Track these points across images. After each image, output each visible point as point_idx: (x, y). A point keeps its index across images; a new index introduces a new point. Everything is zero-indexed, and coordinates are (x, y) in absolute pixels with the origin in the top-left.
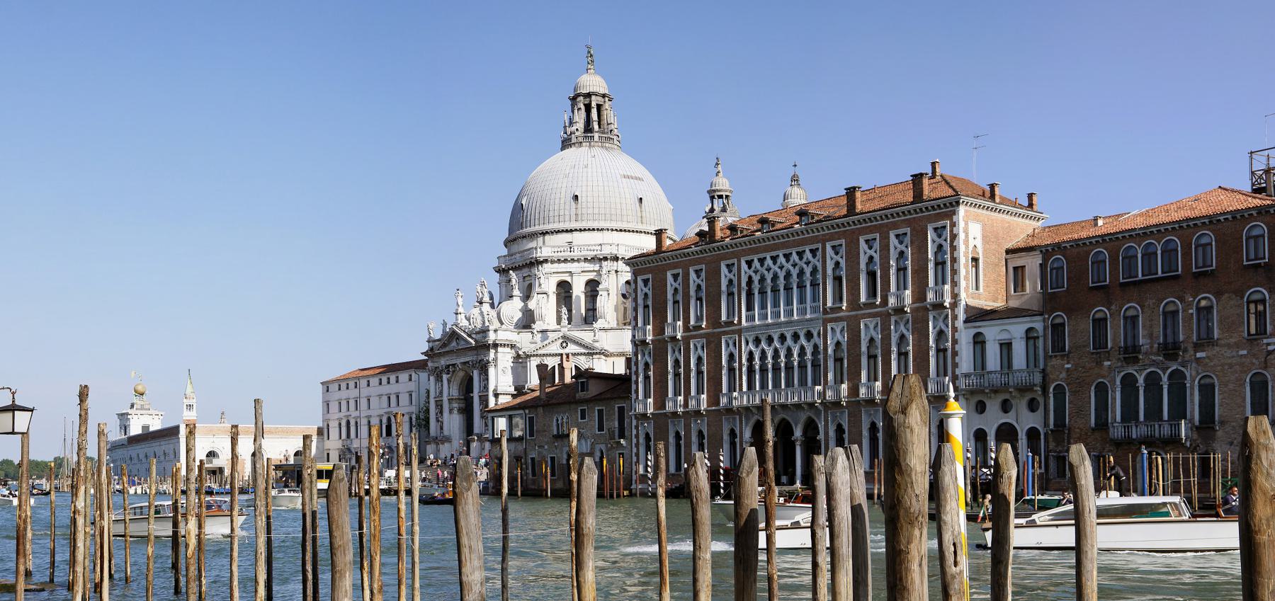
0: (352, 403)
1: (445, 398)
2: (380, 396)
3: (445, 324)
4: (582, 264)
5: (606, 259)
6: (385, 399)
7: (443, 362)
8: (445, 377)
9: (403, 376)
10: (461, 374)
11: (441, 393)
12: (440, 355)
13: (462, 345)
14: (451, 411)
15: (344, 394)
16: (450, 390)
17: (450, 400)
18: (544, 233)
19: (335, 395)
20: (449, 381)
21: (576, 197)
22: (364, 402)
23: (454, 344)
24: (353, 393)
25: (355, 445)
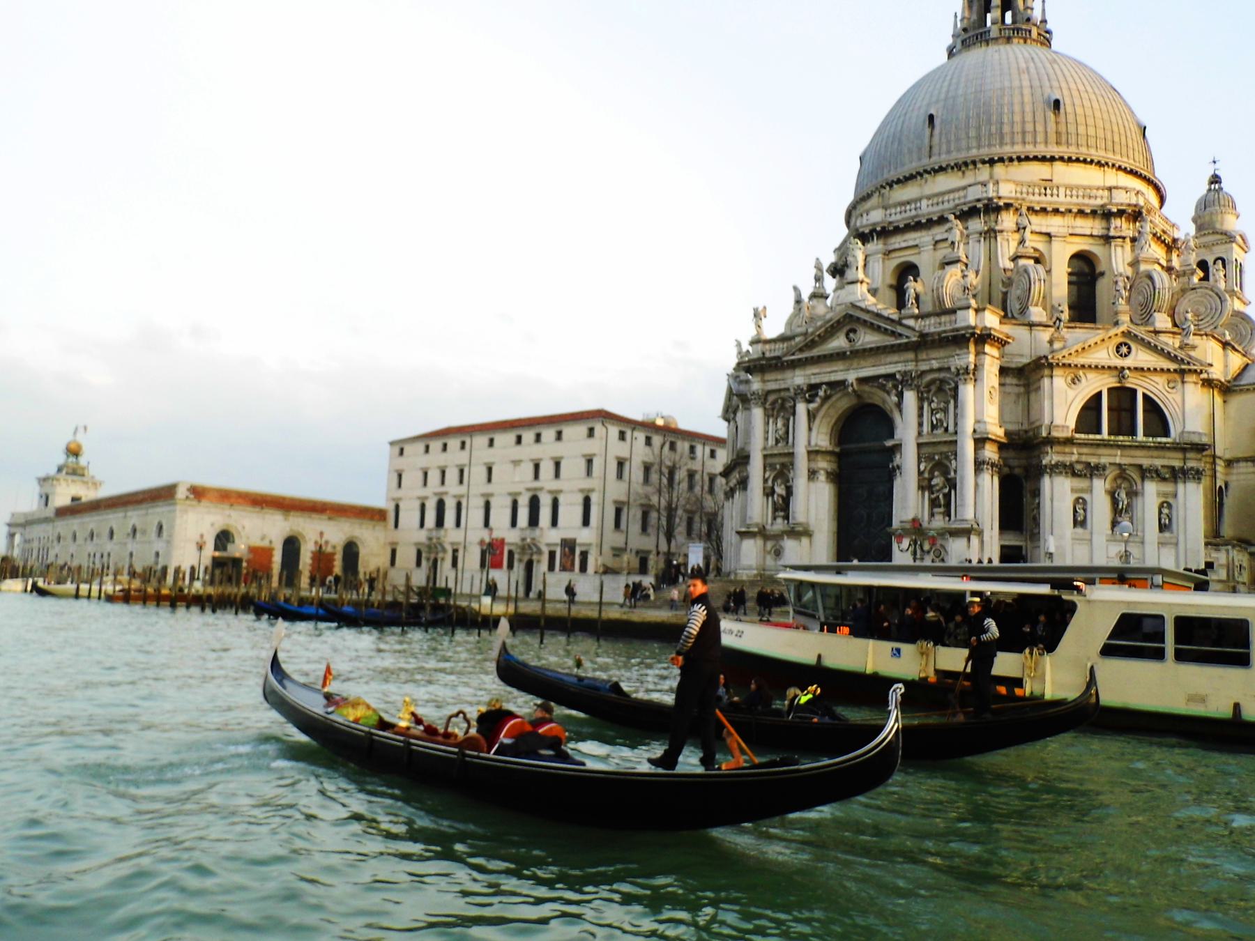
0: (452, 475)
2: (516, 463)
4: (1069, 220)
5: (1121, 213)
7: (799, 378)
8: (801, 408)
9: (574, 432)
10: (843, 404)
12: (794, 365)
13: (867, 339)
14: (812, 474)
15: (436, 458)
16: (811, 434)
17: (813, 454)
18: (992, 162)
20: (811, 416)
21: (1057, 104)
22: (478, 473)
23: (839, 342)
24: (455, 456)
25: (450, 535)
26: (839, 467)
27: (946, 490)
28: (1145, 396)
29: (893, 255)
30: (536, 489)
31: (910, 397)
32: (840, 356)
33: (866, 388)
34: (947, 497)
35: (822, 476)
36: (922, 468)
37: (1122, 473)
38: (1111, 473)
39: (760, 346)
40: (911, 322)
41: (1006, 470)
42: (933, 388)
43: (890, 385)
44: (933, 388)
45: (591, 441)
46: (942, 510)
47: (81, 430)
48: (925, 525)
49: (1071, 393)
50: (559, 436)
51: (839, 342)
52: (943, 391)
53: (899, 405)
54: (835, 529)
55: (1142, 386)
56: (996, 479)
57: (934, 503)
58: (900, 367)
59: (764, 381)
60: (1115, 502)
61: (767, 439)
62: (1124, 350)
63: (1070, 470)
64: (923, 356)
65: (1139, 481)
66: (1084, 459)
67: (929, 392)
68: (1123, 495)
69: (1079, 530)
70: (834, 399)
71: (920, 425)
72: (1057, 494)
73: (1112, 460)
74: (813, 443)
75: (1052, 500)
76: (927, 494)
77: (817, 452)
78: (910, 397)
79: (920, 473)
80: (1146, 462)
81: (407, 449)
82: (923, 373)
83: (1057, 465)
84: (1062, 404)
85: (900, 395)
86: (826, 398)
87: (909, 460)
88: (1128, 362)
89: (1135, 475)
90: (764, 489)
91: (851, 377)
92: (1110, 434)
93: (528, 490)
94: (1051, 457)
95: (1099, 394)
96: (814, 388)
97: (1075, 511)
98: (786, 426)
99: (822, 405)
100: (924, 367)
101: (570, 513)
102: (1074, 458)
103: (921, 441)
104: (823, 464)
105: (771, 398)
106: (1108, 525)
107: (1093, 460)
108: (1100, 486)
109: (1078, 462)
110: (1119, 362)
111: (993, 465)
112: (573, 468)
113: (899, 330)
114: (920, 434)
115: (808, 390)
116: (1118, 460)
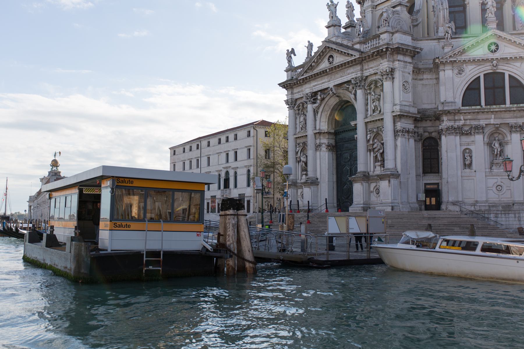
1: (310, 132)
3: (310, 46)
6: (224, 156)
7: (308, 89)
8: (310, 107)
10: (333, 101)
11: (304, 127)
13: (338, 59)
14: (318, 147)
15: (188, 155)
17: (318, 134)
19: (181, 156)
20: (315, 112)
22: (204, 161)
23: (324, 65)
26: (336, 141)
27: (381, 151)
28: (510, 76)
29: (378, 8)
30: (227, 168)
31: (360, 93)
32: (324, 73)
33: (341, 91)
34: (382, 154)
35: (324, 148)
36: (368, 138)
37: (497, 129)
38: (488, 131)
39: (290, 72)
40: (357, 46)
41: (426, 135)
42: (373, 86)
43: (351, 87)
44: (373, 86)
45: (249, 139)
46: (379, 163)
47: (58, 154)
48: (371, 173)
49: (457, 79)
50: (236, 139)
51: (324, 65)
52: (372, 86)
53: (356, 99)
54: (335, 180)
55: (508, 70)
56: (412, 141)
57: (376, 159)
58: (354, 76)
59: (292, 93)
60: (492, 149)
61: (296, 128)
62: (493, 47)
63: (459, 131)
64: (366, 67)
65: (508, 135)
66: (468, 122)
67: (370, 89)
68: (497, 145)
69: (467, 170)
70: (326, 100)
71: (367, 110)
72: (450, 147)
73: (487, 122)
74: (318, 128)
75: (447, 151)
76: (372, 153)
77: (320, 133)
78: (360, 93)
79: (368, 141)
80: (512, 121)
81: (177, 150)
82: (367, 77)
83: (448, 129)
84: (451, 87)
85: (355, 95)
86: (323, 99)
87: (361, 135)
88: (497, 55)
89: (505, 131)
90: (296, 158)
91: (331, 85)
92: (486, 105)
93: (224, 168)
94: (446, 123)
95: (479, 77)
96: (316, 93)
97: (464, 158)
98: (305, 120)
99: (320, 105)
100: (366, 73)
101: (242, 180)
102: (462, 123)
103: (367, 120)
104: (325, 141)
105: (298, 102)
106: (488, 165)
107: (474, 123)
108: (479, 139)
109: (464, 125)
110: (491, 56)
111: (408, 132)
112: (242, 154)
113: (351, 52)
114: (366, 117)
115: (312, 97)
116: (492, 121)
